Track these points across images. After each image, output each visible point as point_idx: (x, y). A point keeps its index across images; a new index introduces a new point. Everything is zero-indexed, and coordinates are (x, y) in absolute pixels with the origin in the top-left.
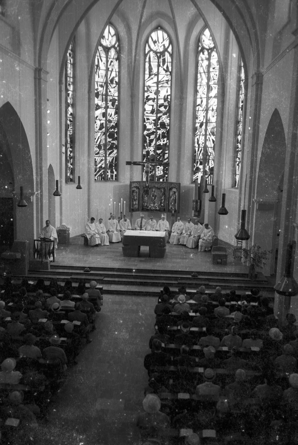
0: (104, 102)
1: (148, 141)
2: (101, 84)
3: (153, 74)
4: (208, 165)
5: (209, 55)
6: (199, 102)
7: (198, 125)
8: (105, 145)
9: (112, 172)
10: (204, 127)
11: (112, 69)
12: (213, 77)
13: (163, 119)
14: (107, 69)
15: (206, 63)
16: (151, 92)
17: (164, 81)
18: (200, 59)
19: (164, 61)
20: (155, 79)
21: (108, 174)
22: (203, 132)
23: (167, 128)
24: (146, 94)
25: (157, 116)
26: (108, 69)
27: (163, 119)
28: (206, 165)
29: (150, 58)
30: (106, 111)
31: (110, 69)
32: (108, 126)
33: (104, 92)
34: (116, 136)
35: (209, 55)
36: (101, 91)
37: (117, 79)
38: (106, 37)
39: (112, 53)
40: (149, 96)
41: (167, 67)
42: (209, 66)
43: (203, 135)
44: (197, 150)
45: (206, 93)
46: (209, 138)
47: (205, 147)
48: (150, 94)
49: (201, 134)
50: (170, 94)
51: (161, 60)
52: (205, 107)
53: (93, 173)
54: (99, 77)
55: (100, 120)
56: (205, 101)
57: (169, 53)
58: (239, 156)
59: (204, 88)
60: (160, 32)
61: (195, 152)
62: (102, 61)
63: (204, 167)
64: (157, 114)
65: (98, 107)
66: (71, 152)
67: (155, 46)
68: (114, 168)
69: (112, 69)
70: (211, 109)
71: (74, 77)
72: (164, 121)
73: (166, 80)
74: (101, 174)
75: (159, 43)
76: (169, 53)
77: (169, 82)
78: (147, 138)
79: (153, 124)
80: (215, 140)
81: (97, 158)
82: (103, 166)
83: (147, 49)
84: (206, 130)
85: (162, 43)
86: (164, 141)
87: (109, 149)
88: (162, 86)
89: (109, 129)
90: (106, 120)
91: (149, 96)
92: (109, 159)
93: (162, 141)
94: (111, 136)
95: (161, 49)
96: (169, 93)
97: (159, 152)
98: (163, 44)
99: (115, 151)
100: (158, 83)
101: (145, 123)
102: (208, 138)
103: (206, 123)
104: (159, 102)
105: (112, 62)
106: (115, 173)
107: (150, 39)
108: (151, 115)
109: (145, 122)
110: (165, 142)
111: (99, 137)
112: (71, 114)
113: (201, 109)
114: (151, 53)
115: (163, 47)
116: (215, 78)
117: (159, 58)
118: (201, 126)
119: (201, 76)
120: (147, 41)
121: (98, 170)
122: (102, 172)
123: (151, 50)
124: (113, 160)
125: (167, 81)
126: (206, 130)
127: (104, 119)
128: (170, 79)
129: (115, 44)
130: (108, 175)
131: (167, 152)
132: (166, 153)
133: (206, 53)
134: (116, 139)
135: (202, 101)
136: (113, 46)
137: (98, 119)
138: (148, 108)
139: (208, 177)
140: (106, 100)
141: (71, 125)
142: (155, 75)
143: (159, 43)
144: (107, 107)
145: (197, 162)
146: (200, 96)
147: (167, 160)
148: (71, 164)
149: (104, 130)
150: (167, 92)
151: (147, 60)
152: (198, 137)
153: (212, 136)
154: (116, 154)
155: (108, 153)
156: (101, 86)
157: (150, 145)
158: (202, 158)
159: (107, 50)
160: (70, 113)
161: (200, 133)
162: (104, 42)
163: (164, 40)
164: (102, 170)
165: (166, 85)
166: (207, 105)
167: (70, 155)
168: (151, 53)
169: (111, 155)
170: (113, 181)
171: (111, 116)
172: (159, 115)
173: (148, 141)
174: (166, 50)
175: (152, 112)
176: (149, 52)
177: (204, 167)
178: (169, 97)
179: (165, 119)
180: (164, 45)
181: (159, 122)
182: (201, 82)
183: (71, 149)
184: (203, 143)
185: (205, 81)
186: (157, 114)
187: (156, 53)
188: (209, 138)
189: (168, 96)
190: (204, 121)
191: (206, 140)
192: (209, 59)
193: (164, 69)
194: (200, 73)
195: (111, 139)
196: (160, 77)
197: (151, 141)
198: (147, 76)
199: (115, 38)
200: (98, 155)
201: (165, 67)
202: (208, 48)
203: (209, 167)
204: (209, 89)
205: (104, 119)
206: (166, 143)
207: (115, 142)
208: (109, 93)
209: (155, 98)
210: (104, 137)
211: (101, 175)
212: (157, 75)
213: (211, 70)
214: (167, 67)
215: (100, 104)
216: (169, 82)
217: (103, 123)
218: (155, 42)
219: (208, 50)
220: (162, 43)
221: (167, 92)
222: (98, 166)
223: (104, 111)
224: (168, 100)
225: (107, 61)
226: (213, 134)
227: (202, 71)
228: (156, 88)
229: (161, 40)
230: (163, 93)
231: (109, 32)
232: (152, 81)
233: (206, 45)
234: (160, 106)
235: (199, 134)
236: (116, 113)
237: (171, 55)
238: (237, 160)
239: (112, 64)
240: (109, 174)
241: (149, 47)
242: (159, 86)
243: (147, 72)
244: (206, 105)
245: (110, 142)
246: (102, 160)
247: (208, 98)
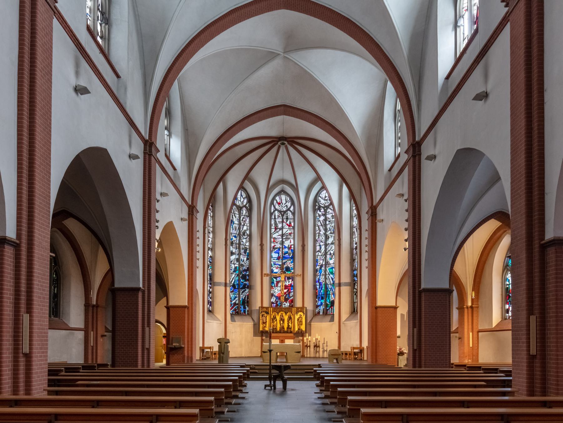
0: (237, 250)
1: (275, 283)
2: (235, 235)
3: (278, 229)
4: (329, 299)
5: (325, 211)
6: (318, 248)
7: (318, 267)
8: (239, 285)
9: (245, 308)
10: (323, 268)
11: (244, 224)
12: (329, 228)
13: (288, 264)
14: (240, 224)
15: (322, 218)
16: (277, 243)
17: (287, 233)
18: (317, 215)
19: (287, 219)
20: (280, 232)
21: (241, 309)
22: (323, 273)
23: (290, 271)
24: (273, 245)
25: (282, 262)
26: (241, 223)
27: (288, 264)
28: (327, 299)
29: (275, 216)
30: (239, 257)
31: (243, 224)
32: (241, 269)
33: (238, 242)
34: (247, 278)
35: (325, 211)
36: (235, 240)
37: (248, 232)
38: (239, 199)
39: (244, 211)
40: (275, 246)
41: (290, 223)
42: (325, 220)
43: (323, 275)
44: (318, 288)
45: (324, 241)
46: (328, 277)
47: (326, 284)
48: (276, 244)
49: (322, 274)
50: (293, 244)
51: (285, 217)
52: (323, 252)
53: (229, 307)
54: (233, 230)
55: (234, 264)
56: (323, 247)
57: (291, 211)
58: (356, 287)
59: (322, 237)
60: (283, 197)
61: (317, 290)
62: (235, 217)
63: (326, 301)
64: (282, 260)
65: (232, 253)
66: (210, 288)
67: (279, 207)
68: (246, 304)
69: (244, 224)
70: (329, 253)
71: (214, 227)
72: (289, 265)
73: (289, 233)
74: (235, 309)
75: (282, 204)
76: (291, 211)
77: (292, 235)
78: (275, 280)
79: (279, 269)
80: (333, 278)
81: (231, 295)
82: (237, 302)
83: (273, 208)
84: (325, 271)
85: (285, 204)
86: (289, 282)
87: (241, 289)
88: (285, 238)
89: (242, 272)
90: (239, 264)
91: (275, 246)
92: (242, 296)
93: (288, 282)
94: (244, 277)
95: (285, 209)
96: (292, 243)
97: (285, 291)
98: (285, 205)
99: (247, 290)
100: (282, 235)
101: (272, 268)
102: (327, 277)
103: (326, 265)
104: (283, 251)
105: (243, 218)
106: (247, 309)
107: (275, 202)
108: (278, 261)
109: (272, 267)
110: (290, 283)
111: (233, 278)
112: (211, 257)
113: (320, 254)
114: (276, 212)
115: (285, 207)
116: (331, 229)
117: (283, 216)
118: (321, 268)
119: (319, 228)
120: (272, 203)
121: (232, 305)
122: (236, 308)
123: (276, 210)
124: (245, 297)
125: (290, 234)
126: (325, 271)
127: (238, 263)
128: (293, 232)
129: (246, 204)
130: (241, 310)
131: (292, 291)
132: (292, 292)
133: (322, 210)
134: (248, 280)
135: (321, 248)
136: (245, 206)
137: (232, 263)
138: (275, 255)
139: (329, 308)
140: (239, 248)
141: (211, 265)
142: (280, 229)
143: (282, 204)
144: (239, 254)
145: (319, 298)
146: (319, 244)
147: (292, 298)
148: (210, 298)
149: (237, 272)
150: (290, 242)
151: (273, 217)
152: (318, 277)
153: (331, 275)
154: (248, 293)
155: (241, 292)
156: (235, 237)
157: (277, 286)
158: (323, 294)
159: (240, 209)
160: (209, 256)
161: (321, 274)
162: (238, 203)
163: (286, 202)
164: (236, 306)
165: (289, 237)
166: (326, 249)
167: (209, 290)
168: (276, 212)
169: (244, 294)
170: (245, 315)
171: (243, 261)
172: (284, 261)
173: (275, 283)
174: (289, 209)
175: (278, 258)
176: (274, 211)
177: (326, 301)
178: (292, 247)
179: (289, 264)
180: (287, 206)
181: (285, 266)
182: (319, 233)
183: (210, 286)
184: (323, 281)
185: (322, 232)
186: (282, 260)
187: (280, 212)
188: (328, 277)
189: (291, 245)
190: (324, 263)
191: (326, 278)
192: (325, 215)
193: (287, 224)
194: (318, 226)
195: (244, 280)
196: (285, 231)
197: (278, 282)
198: (273, 230)
199: (246, 201)
200: (233, 293)
201: (288, 223)
202: (323, 206)
203: (330, 300)
204: (327, 238)
205: (238, 263)
206: (291, 284)
207: (247, 283)
208: (242, 243)
209: (280, 248)
210: (237, 278)
211: (235, 310)
212: (282, 229)
213: (328, 223)
214: (290, 223)
215: (234, 251)
216: (292, 235)
217: (237, 267)
218: (279, 204)
219: (324, 208)
220: (285, 204)
221: (290, 242)
222: (233, 302)
223: (237, 257)
224: (291, 249)
225: (240, 217)
226: (332, 273)
227: (319, 224)
228: (281, 240)
229: (284, 202)
230: (287, 244)
231: (241, 195)
232: (277, 234)
233: (322, 204)
234: (285, 254)
235: (319, 274)
236: (247, 259)
237: (294, 214)
238: (355, 290)
239: (244, 220)
240: (242, 309)
241: (274, 207)
242: (284, 237)
243: (273, 227)
244: (325, 250)
245: (243, 282)
246: (236, 297)
247: (326, 245)
